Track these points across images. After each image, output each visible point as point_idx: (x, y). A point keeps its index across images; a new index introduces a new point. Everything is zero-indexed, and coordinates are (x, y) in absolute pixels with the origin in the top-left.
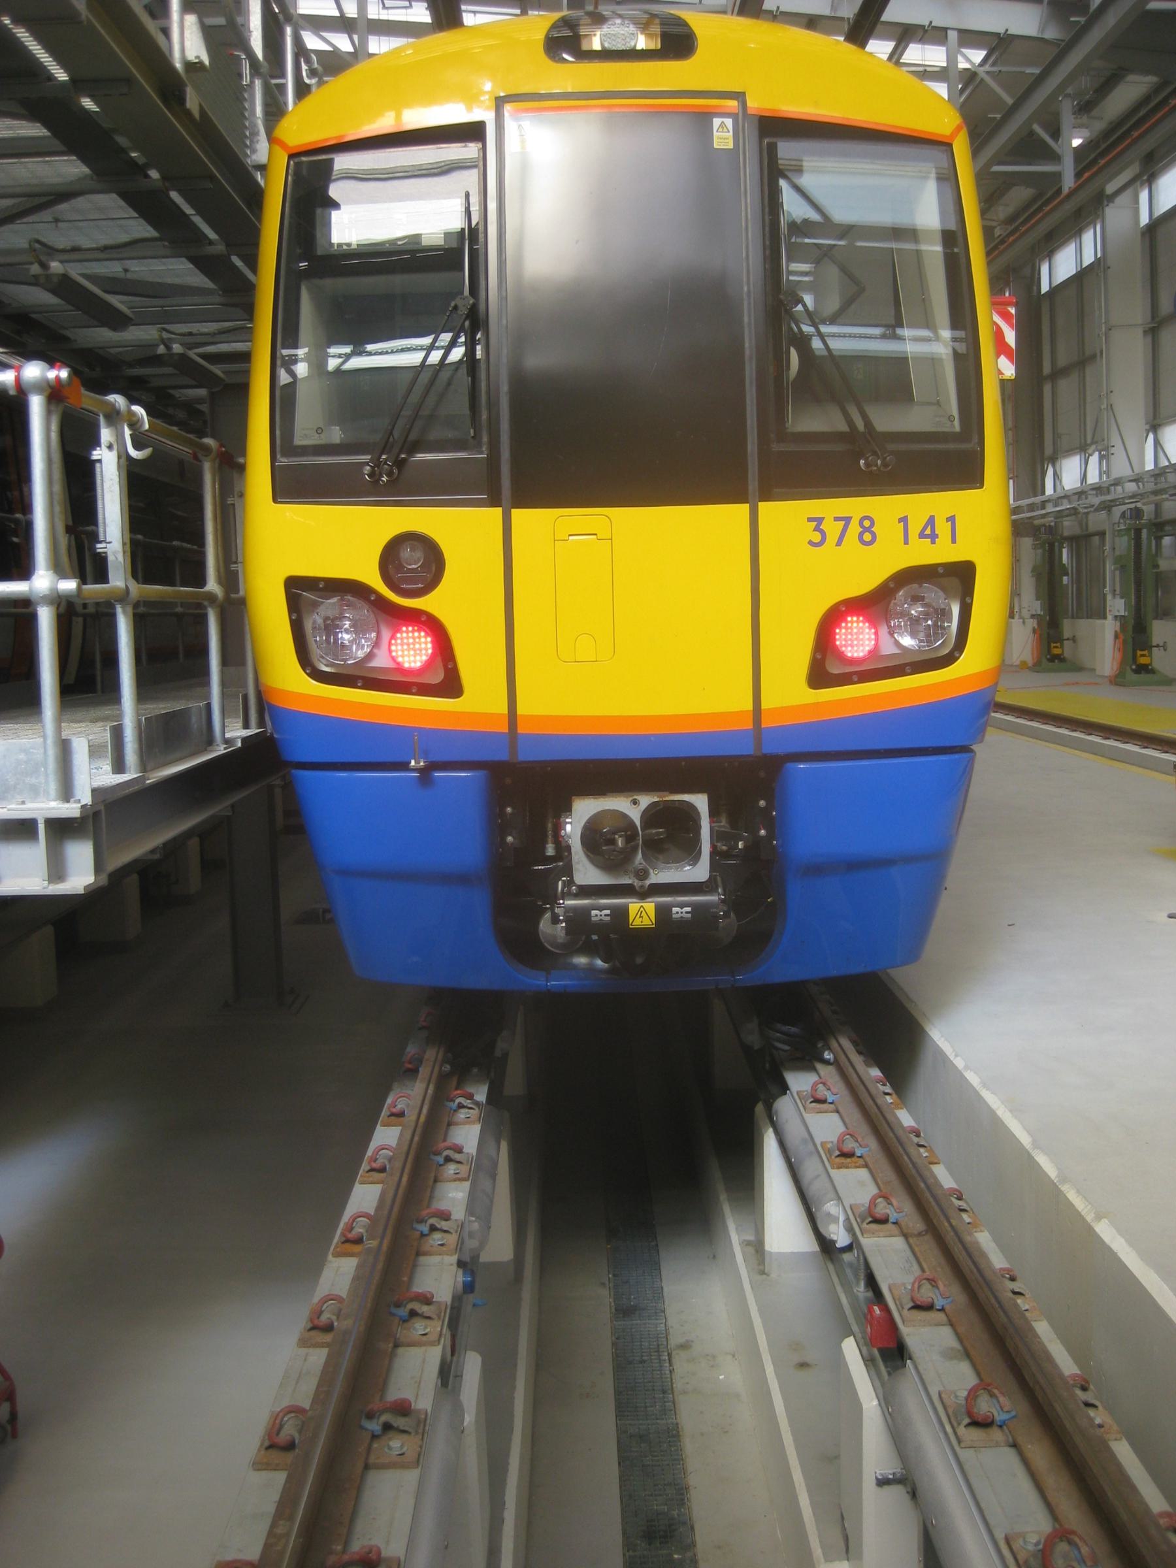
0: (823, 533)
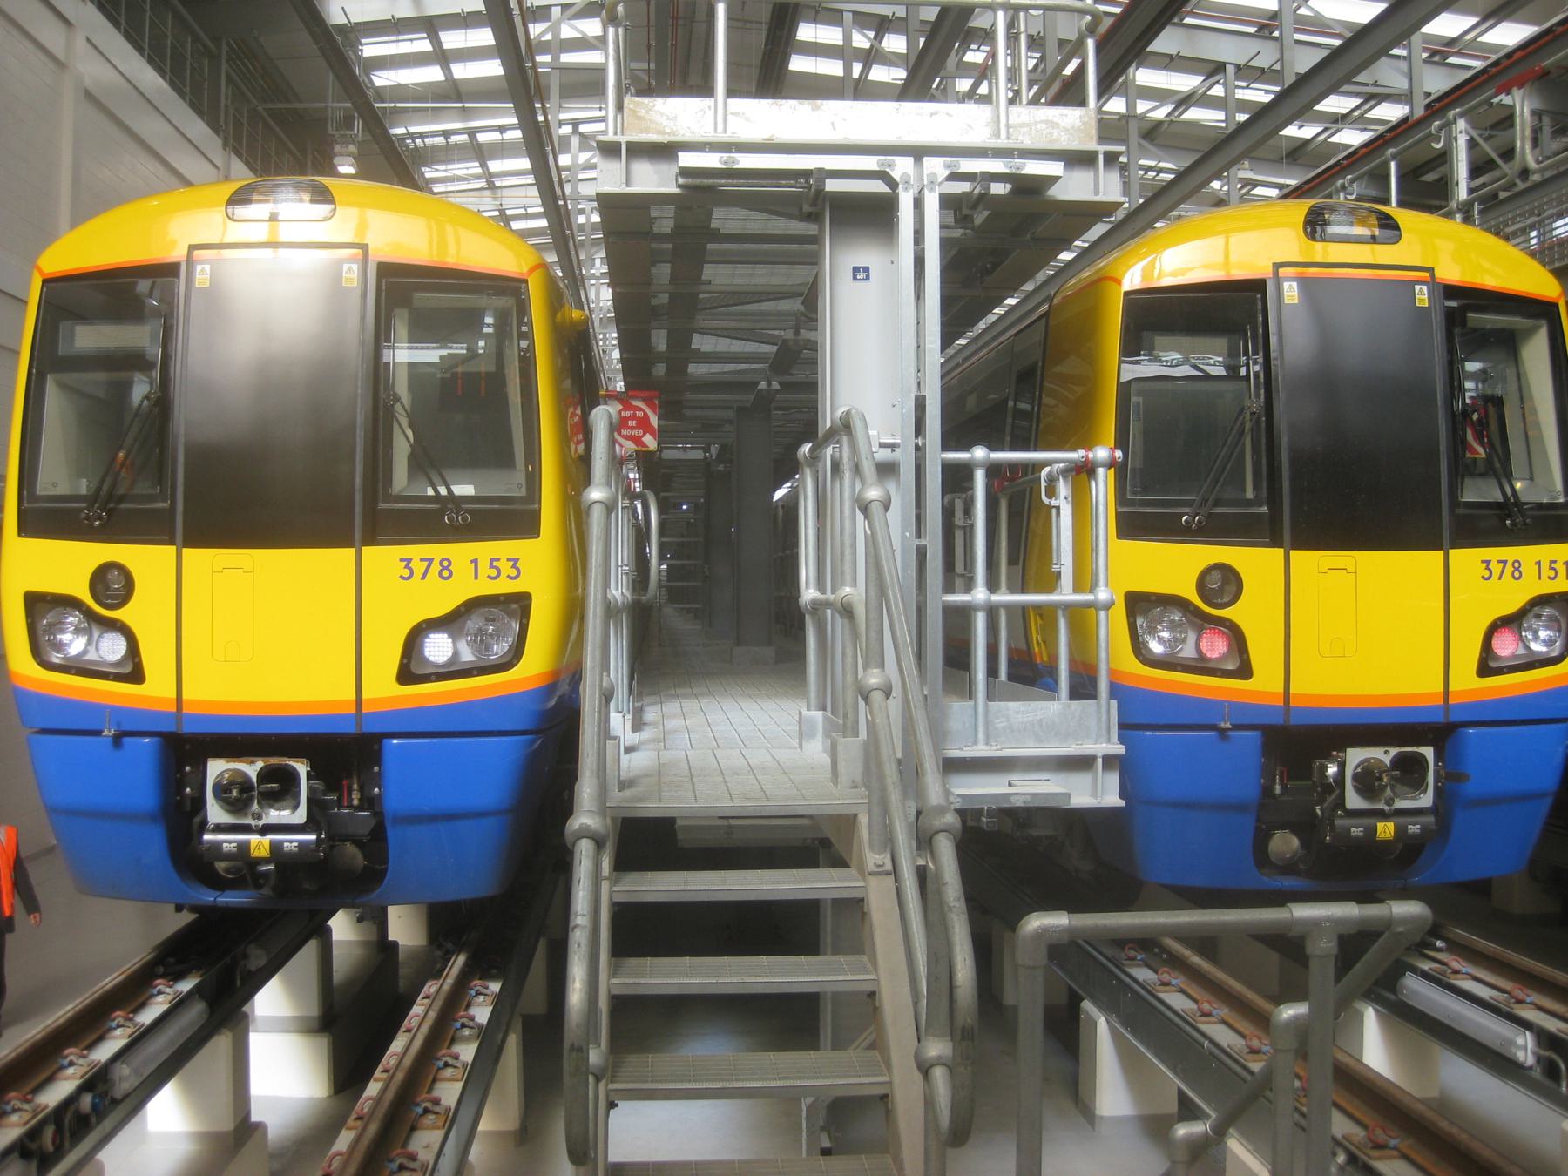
0: (499, 570)
